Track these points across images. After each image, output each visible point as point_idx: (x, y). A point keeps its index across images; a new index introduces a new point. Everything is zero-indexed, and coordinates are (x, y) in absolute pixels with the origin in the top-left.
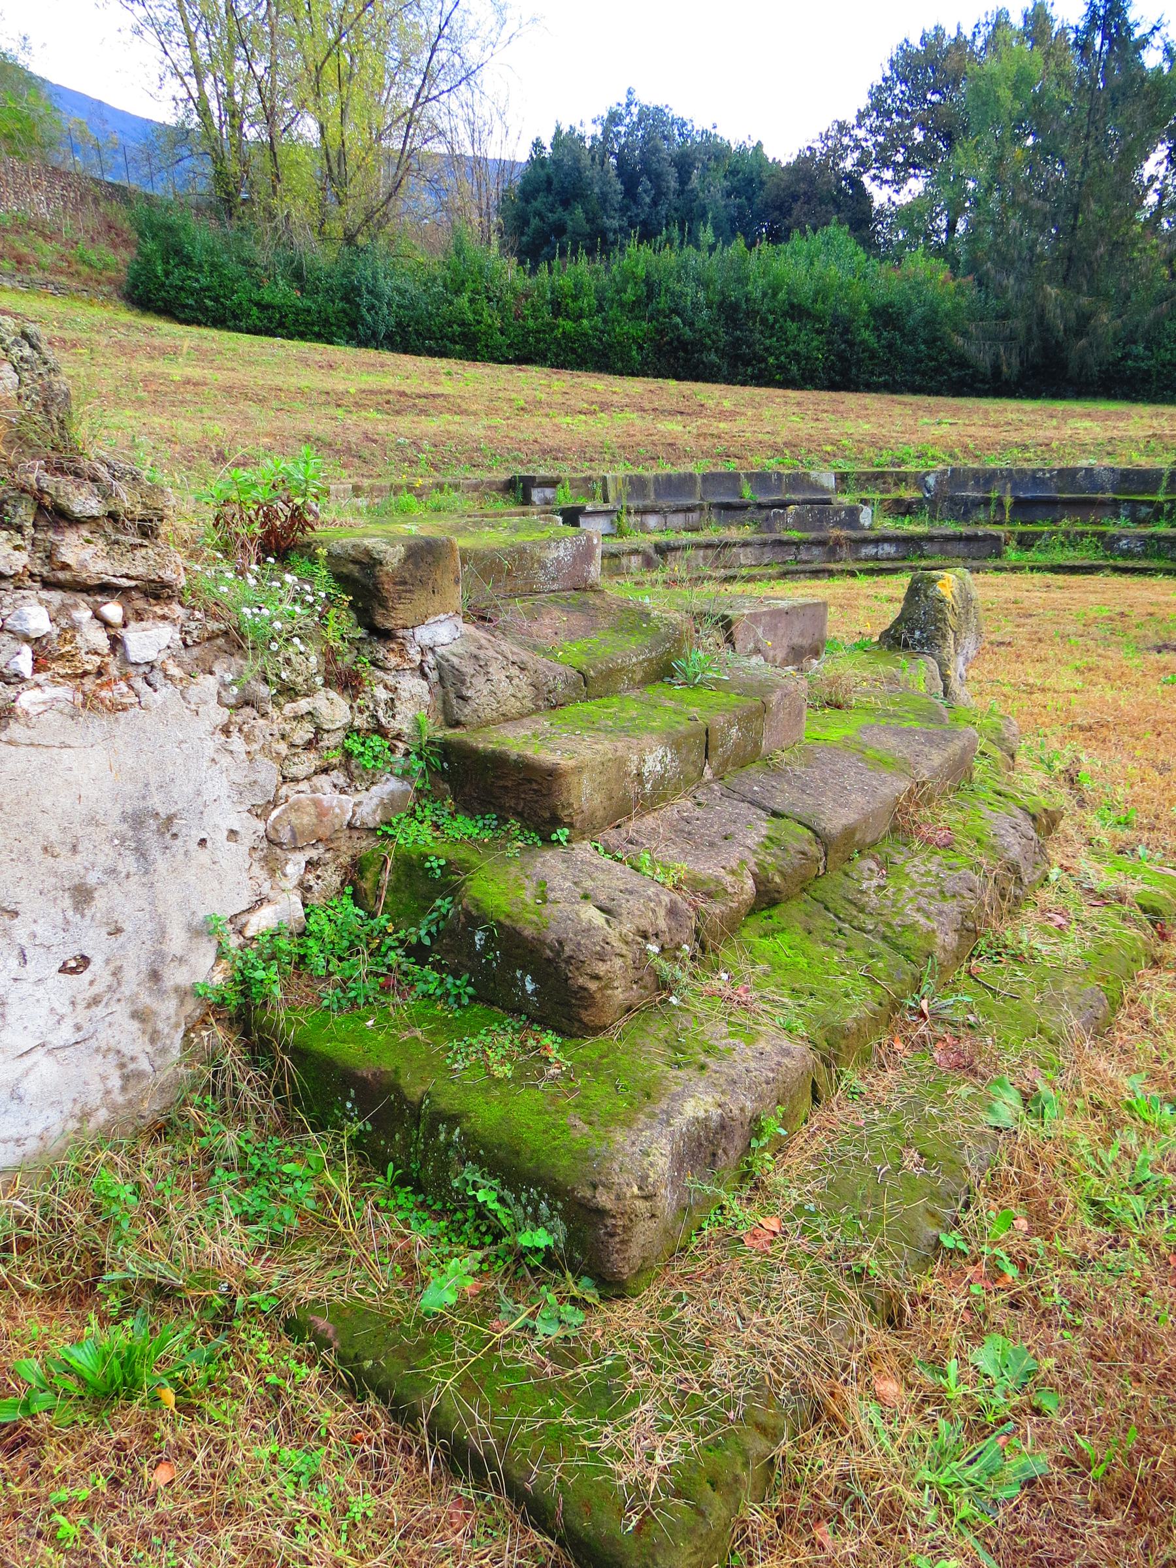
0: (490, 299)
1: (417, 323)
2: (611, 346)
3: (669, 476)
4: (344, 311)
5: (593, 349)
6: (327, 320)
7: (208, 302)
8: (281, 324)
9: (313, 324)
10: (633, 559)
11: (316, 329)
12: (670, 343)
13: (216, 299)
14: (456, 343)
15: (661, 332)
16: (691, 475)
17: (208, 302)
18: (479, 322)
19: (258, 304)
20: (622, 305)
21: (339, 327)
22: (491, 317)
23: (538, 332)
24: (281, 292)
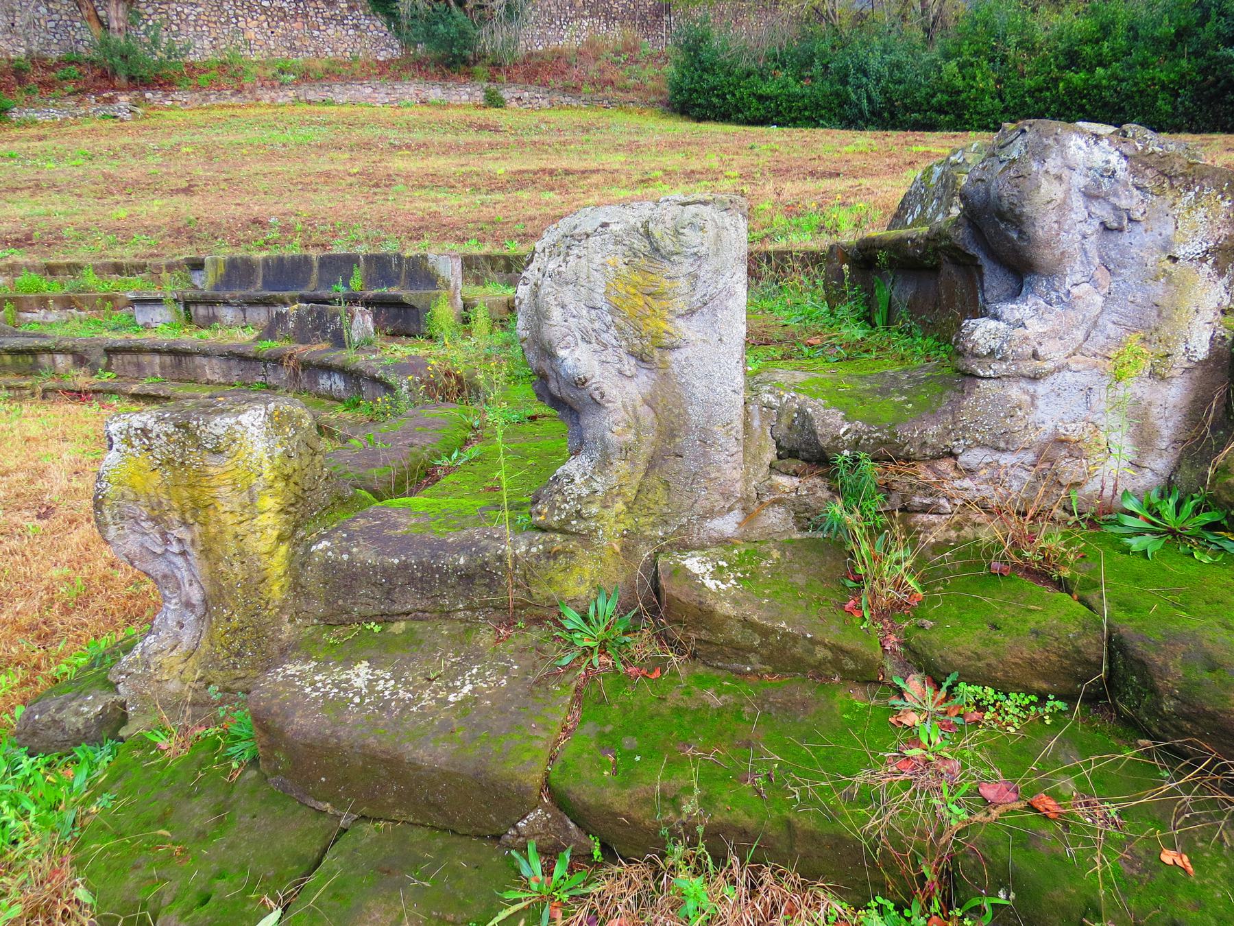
0: (992, 60)
1: (906, 96)
2: (1129, 97)
3: (281, 260)
4: (837, 94)
5: (1106, 105)
6: (818, 105)
7: (715, 100)
8: (779, 113)
9: (806, 109)
10: (59, 359)
11: (807, 113)
12: (1214, 84)
13: (723, 97)
14: (946, 113)
15: (1203, 71)
16: (306, 257)
17: (715, 100)
18: (972, 87)
19: (761, 98)
20: (1157, 41)
21: (831, 110)
22: (985, 78)
23: (1040, 90)
24: (780, 83)
